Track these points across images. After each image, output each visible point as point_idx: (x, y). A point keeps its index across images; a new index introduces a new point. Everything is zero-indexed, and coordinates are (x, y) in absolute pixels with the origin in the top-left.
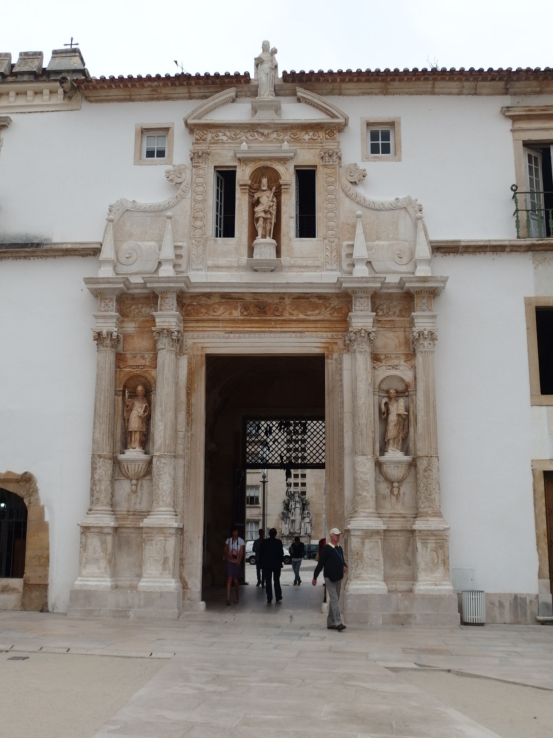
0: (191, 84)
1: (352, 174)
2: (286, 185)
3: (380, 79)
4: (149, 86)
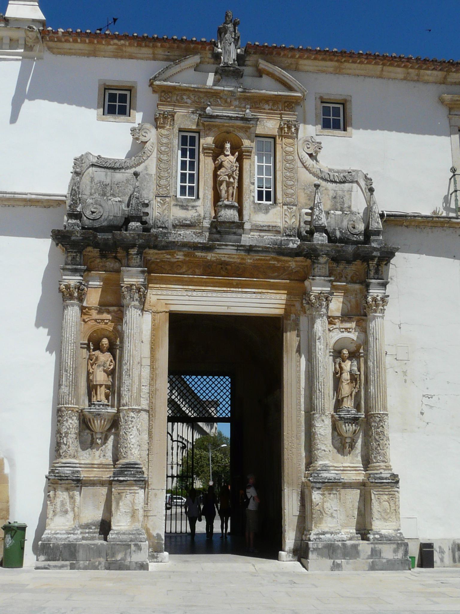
0: (156, 47)
1: (308, 146)
2: (248, 152)
3: (336, 59)
4: (114, 44)
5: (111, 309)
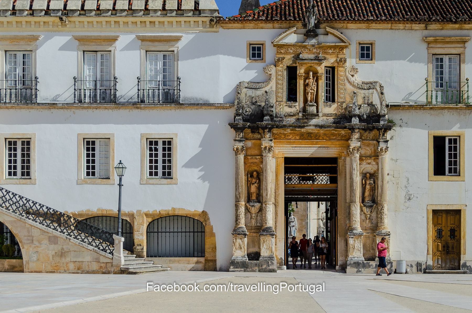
5: (257, 157)
